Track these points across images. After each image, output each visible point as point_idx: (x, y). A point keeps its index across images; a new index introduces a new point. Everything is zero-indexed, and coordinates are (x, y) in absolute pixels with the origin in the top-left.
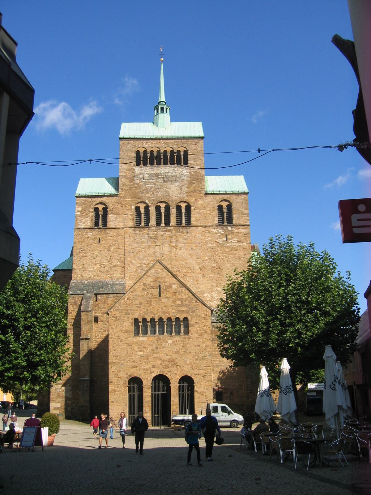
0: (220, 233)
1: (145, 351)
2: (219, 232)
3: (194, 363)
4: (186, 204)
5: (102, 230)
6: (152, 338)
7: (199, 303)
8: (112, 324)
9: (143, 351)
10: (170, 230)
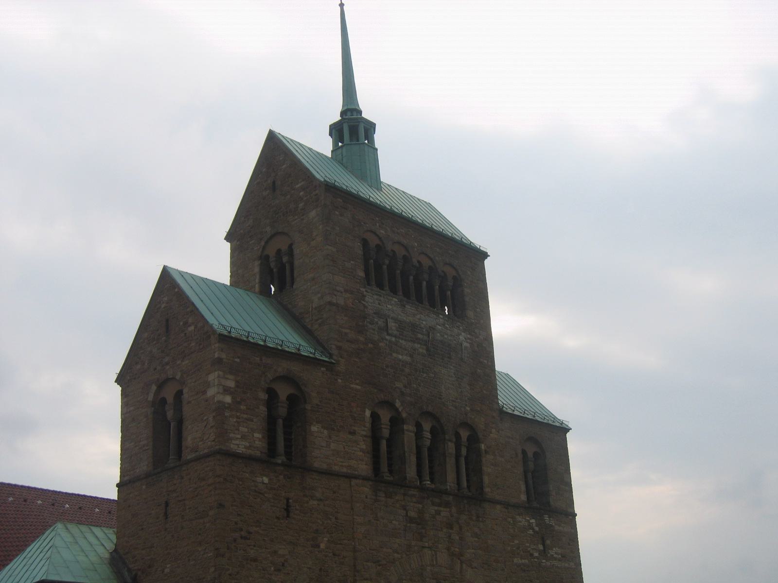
0: (533, 529)
2: (530, 525)
10: (447, 505)
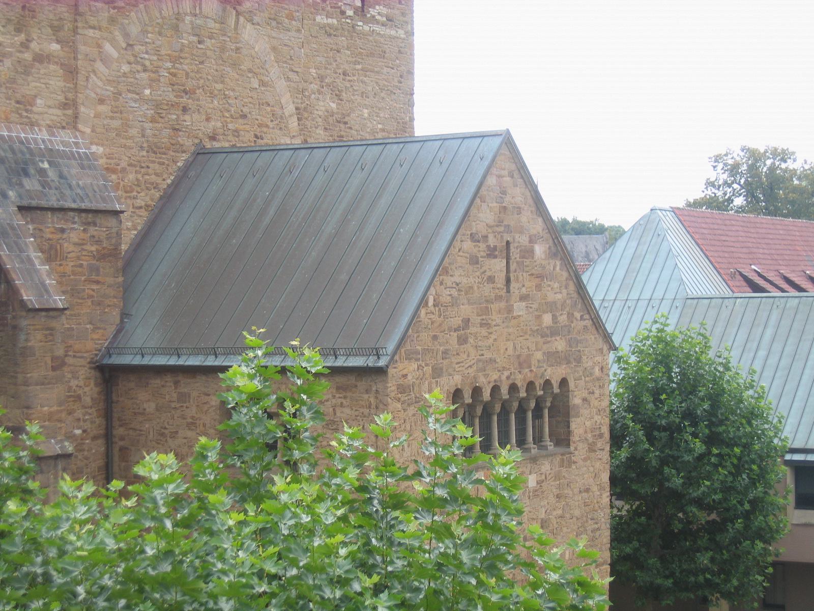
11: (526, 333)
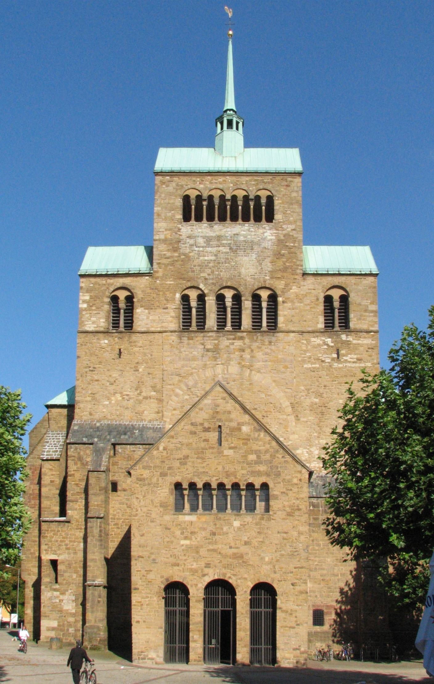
1: (194, 539)
3: (277, 561)
4: (268, 293)
5: (124, 334)
6: (205, 516)
7: (288, 458)
8: (136, 492)
9: (191, 539)
11: (233, 462)
